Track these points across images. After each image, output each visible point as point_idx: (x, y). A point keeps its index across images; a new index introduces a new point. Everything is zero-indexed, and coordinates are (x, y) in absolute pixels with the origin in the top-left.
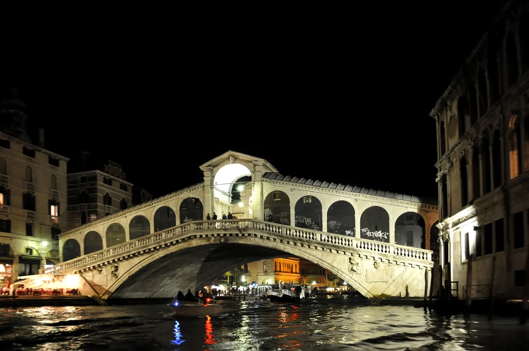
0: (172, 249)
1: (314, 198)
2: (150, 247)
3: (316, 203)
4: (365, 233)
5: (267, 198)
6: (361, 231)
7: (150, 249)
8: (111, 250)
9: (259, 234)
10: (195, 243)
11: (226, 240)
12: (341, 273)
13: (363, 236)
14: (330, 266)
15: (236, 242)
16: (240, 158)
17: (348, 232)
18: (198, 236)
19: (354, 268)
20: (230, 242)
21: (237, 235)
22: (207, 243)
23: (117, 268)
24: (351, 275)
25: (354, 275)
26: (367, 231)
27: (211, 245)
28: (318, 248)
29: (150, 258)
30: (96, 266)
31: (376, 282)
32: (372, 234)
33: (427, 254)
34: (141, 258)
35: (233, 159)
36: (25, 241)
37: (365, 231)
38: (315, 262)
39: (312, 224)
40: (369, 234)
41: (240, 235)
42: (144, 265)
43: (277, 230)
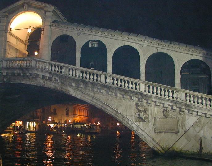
1: (100, 43)
3: (102, 48)
9: (41, 74)
12: (126, 120)
14: (114, 112)
15: (19, 82)
16: (33, 5)
19: (141, 116)
21: (19, 74)
24: (137, 123)
28: (102, 91)
31: (165, 132)
38: (99, 107)
43: (60, 70)
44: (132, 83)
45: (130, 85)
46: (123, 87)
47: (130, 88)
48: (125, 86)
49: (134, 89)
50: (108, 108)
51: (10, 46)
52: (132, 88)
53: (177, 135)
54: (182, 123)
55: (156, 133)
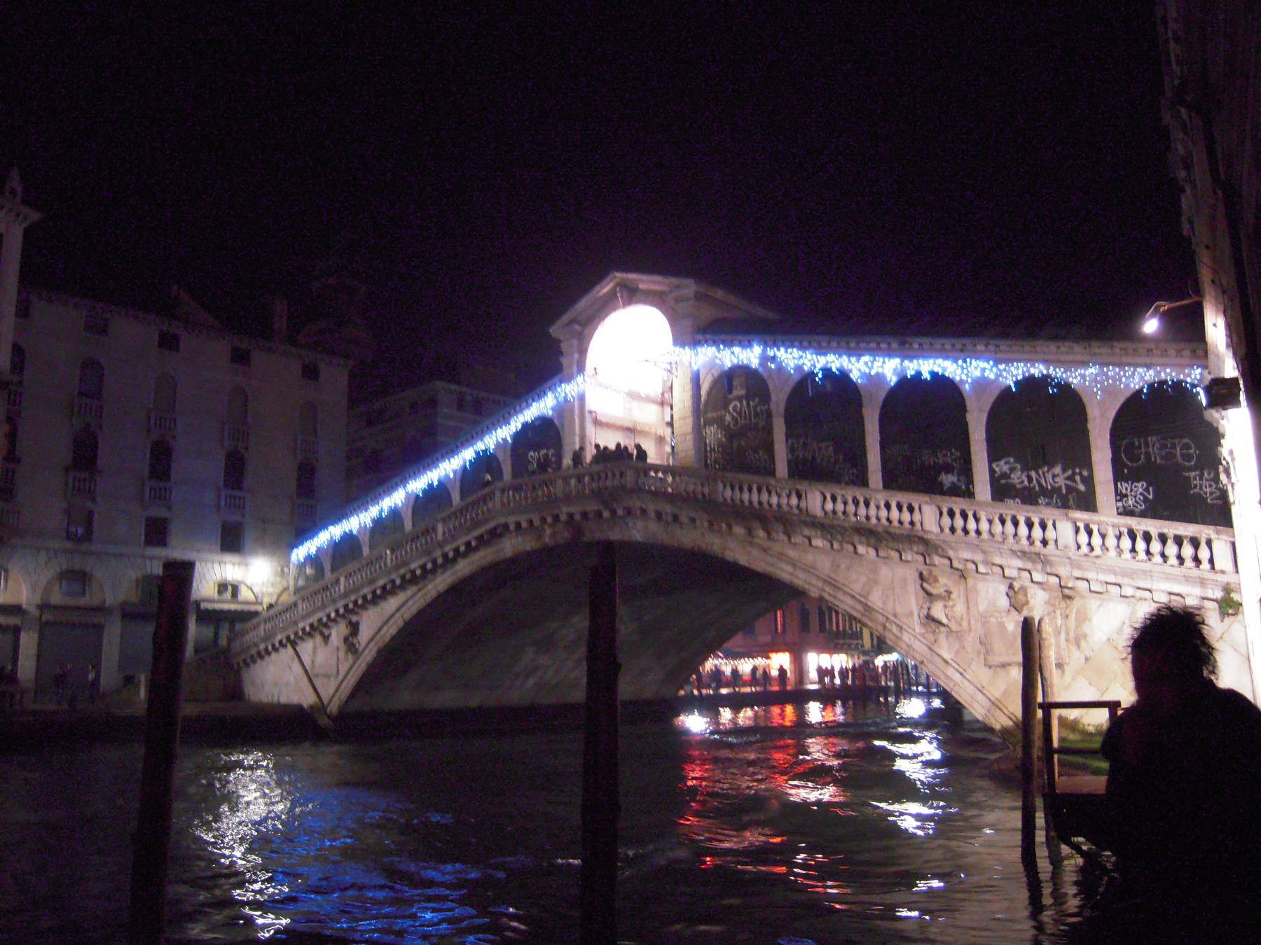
0: (463, 568)
4: (1005, 476)
5: (709, 393)
6: (992, 471)
7: (413, 572)
8: (342, 579)
9: (651, 508)
10: (509, 546)
11: (579, 531)
12: (894, 629)
13: (1001, 491)
14: (858, 607)
17: (948, 479)
18: (512, 527)
20: (588, 537)
23: (354, 628)
25: (942, 638)
26: (1012, 469)
27: (546, 551)
29: (420, 595)
30: (316, 624)
32: (1030, 479)
33: (1209, 543)
34: (402, 597)
35: (625, 293)
37: (1006, 468)
39: (836, 462)
40: (1019, 478)
41: (606, 514)
42: (407, 616)
44: (900, 507)
45: (895, 513)
46: (874, 521)
47: (896, 523)
48: (878, 519)
49: (907, 525)
50: (840, 595)
51: (597, 423)
52: (900, 522)
54: (1077, 627)
55: (990, 667)
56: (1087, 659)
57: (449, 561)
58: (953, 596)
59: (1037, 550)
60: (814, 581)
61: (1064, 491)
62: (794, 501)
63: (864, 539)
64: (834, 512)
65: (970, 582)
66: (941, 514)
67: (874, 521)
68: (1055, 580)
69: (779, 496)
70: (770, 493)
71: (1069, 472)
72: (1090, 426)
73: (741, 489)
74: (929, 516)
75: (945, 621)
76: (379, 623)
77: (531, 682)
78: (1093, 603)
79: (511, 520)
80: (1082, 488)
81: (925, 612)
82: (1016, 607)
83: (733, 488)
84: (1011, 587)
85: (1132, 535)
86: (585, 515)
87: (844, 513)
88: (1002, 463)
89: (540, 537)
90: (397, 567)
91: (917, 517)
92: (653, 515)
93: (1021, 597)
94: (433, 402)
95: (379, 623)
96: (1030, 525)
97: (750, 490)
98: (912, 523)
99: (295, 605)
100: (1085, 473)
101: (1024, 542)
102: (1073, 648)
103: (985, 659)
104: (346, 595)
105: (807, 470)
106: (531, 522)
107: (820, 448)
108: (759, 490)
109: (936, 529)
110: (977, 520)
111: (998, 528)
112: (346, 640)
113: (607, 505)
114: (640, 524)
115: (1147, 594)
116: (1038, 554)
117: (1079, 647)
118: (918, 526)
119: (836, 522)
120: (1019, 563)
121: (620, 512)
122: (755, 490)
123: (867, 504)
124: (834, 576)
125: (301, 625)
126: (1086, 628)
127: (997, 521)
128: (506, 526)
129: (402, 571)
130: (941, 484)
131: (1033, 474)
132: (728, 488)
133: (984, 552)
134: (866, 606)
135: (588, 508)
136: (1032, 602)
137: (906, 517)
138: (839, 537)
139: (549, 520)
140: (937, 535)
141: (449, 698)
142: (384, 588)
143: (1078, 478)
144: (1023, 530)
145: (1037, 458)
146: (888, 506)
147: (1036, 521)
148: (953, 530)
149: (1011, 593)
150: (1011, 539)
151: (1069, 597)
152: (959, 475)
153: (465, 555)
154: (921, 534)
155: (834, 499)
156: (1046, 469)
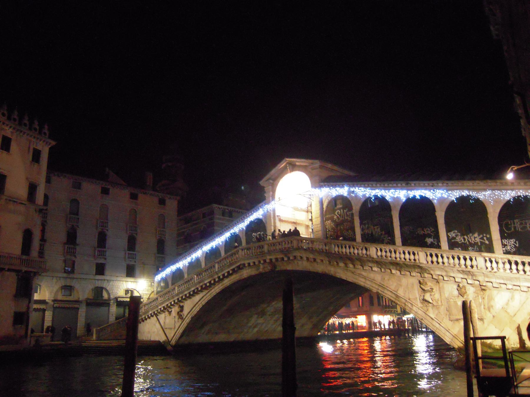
0: (227, 282)
2: (206, 282)
4: (454, 238)
5: (327, 207)
6: (448, 237)
7: (206, 284)
8: (176, 288)
9: (304, 256)
10: (246, 273)
11: (274, 266)
12: (410, 305)
13: (453, 245)
14: (393, 296)
17: (429, 240)
18: (247, 265)
20: (278, 269)
21: (283, 259)
22: (257, 272)
23: (182, 308)
25: (430, 309)
26: (456, 236)
27: (261, 274)
28: (374, 269)
29: (209, 294)
30: (166, 307)
32: (464, 239)
34: (201, 295)
35: (291, 167)
36: (124, 283)
37: (454, 235)
39: (381, 234)
40: (459, 239)
41: (286, 259)
42: (204, 303)
44: (409, 253)
45: (407, 256)
46: (398, 259)
47: (408, 260)
48: (400, 258)
49: (412, 261)
50: (386, 291)
51: (281, 220)
52: (410, 260)
53: (484, 323)
54: (488, 304)
55: (451, 321)
56: (494, 316)
57: (220, 280)
58: (434, 291)
59: (469, 270)
60: (374, 285)
61: (479, 244)
62: (364, 252)
63: (395, 267)
64: (381, 256)
65: (441, 284)
66: (427, 255)
67: (398, 259)
68: (477, 283)
69: (358, 249)
70: (354, 248)
71: (481, 236)
72: (489, 216)
73: (342, 247)
74: (422, 256)
75: (431, 301)
76: (192, 306)
77: (256, 330)
78: (495, 292)
79: (246, 262)
80: (487, 242)
81: (422, 297)
82: (461, 294)
83: (338, 247)
84: (459, 286)
85: (510, 263)
86: (277, 259)
87: (386, 256)
88: (452, 233)
89: (258, 269)
90: (200, 282)
91: (417, 257)
92: (305, 259)
93: (463, 290)
94: (212, 213)
95: (192, 306)
96: (465, 259)
97: (346, 247)
98: (415, 260)
99: (157, 299)
100: (488, 236)
101: (463, 266)
102: (487, 312)
103: (450, 318)
104: (177, 295)
105: (369, 239)
106: (254, 263)
107: (374, 229)
108: (350, 248)
109: (425, 262)
110: (442, 257)
111: (451, 261)
112: (178, 313)
113: (286, 256)
114: (300, 263)
115: (518, 288)
116: (469, 272)
117: (490, 311)
118: (417, 261)
119: (382, 260)
120: (462, 276)
121: (291, 258)
122: (348, 247)
123: (395, 252)
124: (382, 283)
125: (159, 307)
126: (492, 303)
127: (451, 258)
128: (244, 264)
129: (201, 284)
130: (426, 242)
131: (466, 237)
132: (336, 246)
133: (446, 271)
134: (397, 296)
135: (278, 257)
136: (468, 292)
137: (412, 257)
138: (384, 266)
139: (262, 262)
140: (426, 265)
141: (222, 337)
142: (194, 291)
143: (485, 238)
144: (462, 261)
145: (467, 230)
146: (404, 253)
147: (468, 257)
148: (432, 262)
149: (459, 289)
150: (457, 266)
151: (484, 290)
152: (434, 238)
153: (227, 277)
154: (419, 264)
155: (381, 250)
156: (471, 235)
